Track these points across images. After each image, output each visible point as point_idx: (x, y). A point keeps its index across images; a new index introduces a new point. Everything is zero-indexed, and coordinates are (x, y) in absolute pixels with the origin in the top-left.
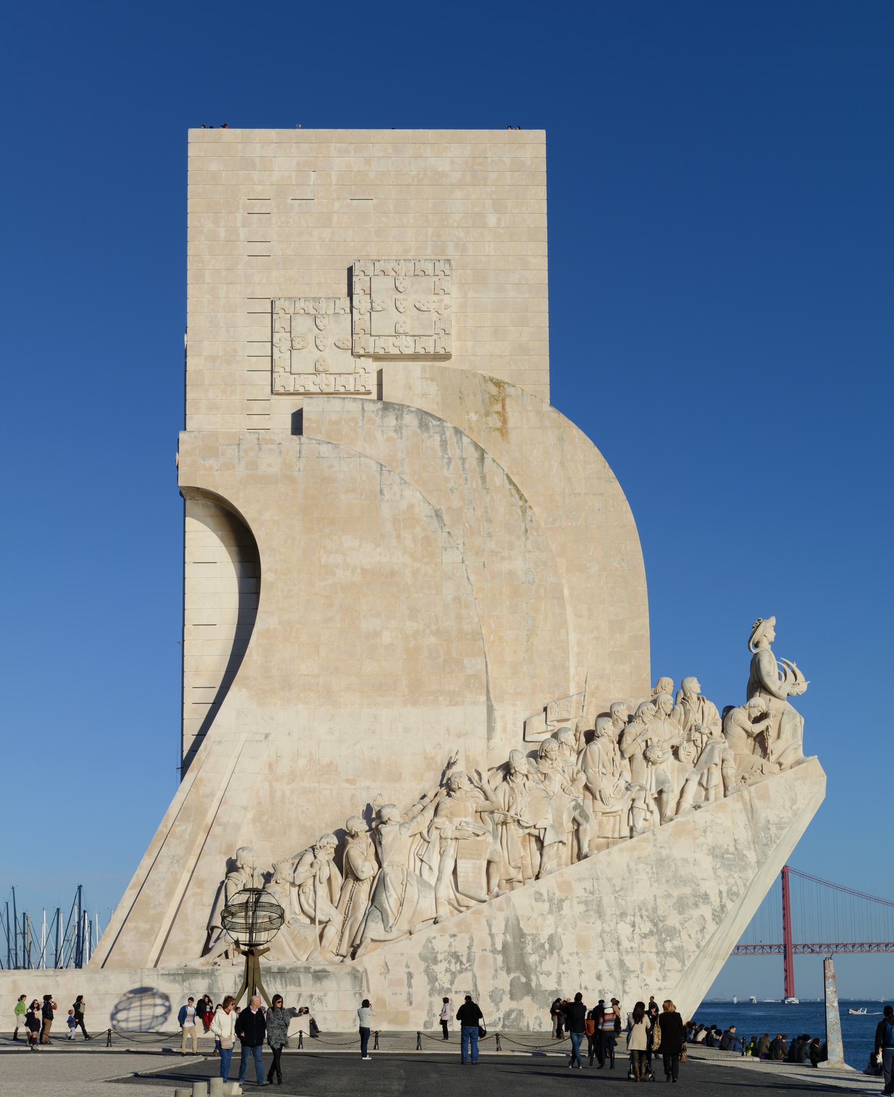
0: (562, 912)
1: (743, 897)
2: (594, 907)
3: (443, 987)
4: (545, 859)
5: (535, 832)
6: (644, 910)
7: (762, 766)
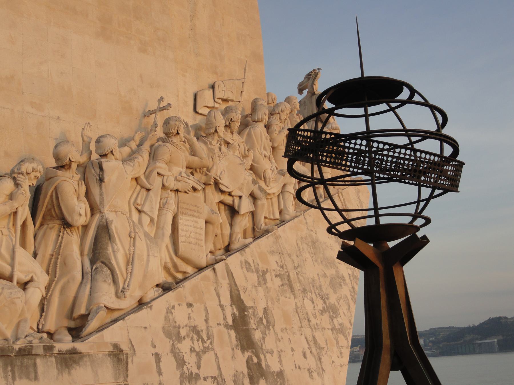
0: (268, 285)
2: (287, 282)
3: (192, 373)
5: (228, 200)
6: (315, 288)
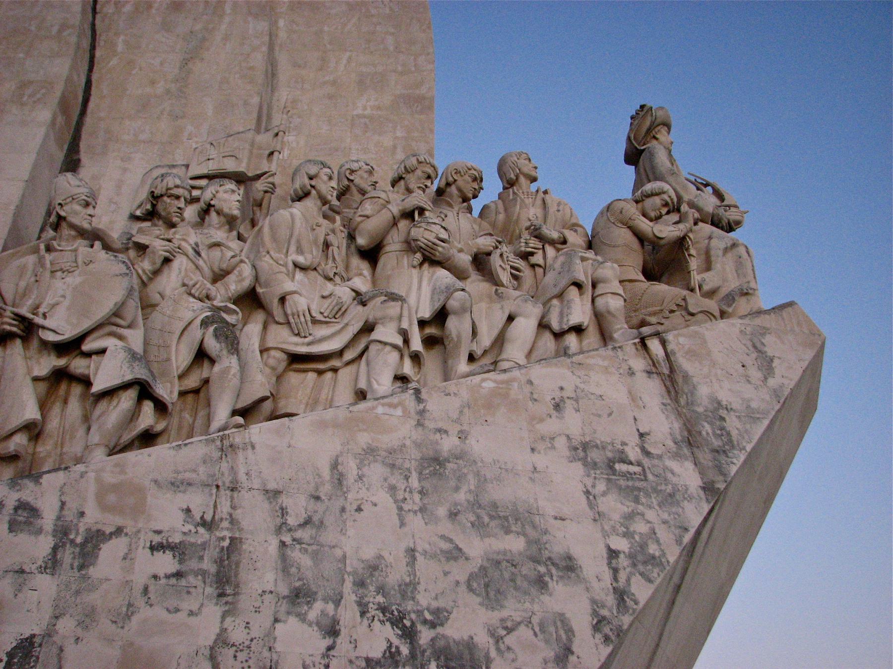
0: (92, 571)
1: (676, 579)
2: (208, 565)
4: (95, 437)
6: (372, 588)
7: (684, 299)
